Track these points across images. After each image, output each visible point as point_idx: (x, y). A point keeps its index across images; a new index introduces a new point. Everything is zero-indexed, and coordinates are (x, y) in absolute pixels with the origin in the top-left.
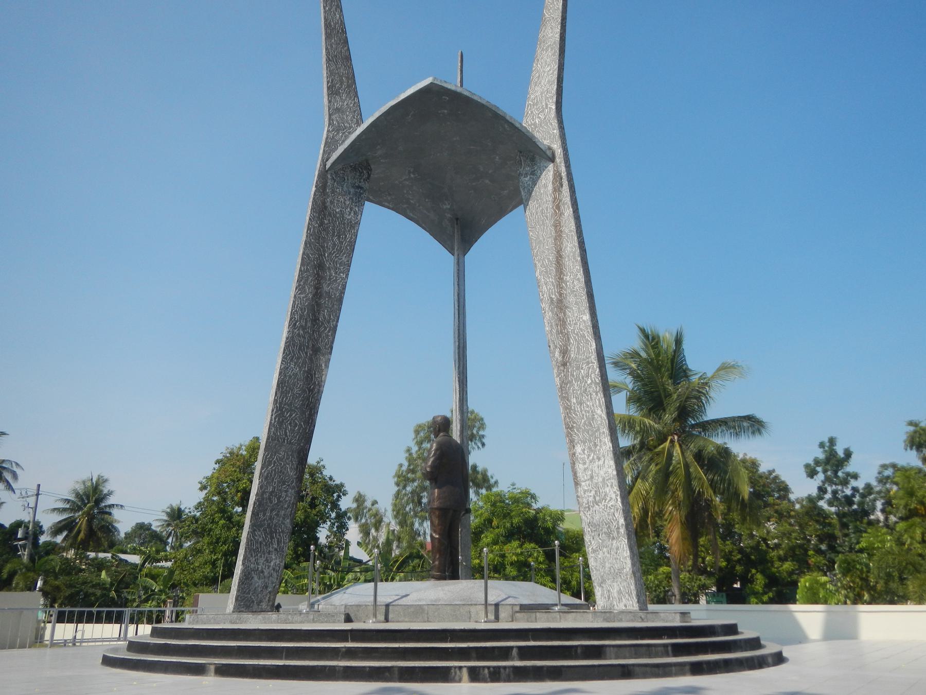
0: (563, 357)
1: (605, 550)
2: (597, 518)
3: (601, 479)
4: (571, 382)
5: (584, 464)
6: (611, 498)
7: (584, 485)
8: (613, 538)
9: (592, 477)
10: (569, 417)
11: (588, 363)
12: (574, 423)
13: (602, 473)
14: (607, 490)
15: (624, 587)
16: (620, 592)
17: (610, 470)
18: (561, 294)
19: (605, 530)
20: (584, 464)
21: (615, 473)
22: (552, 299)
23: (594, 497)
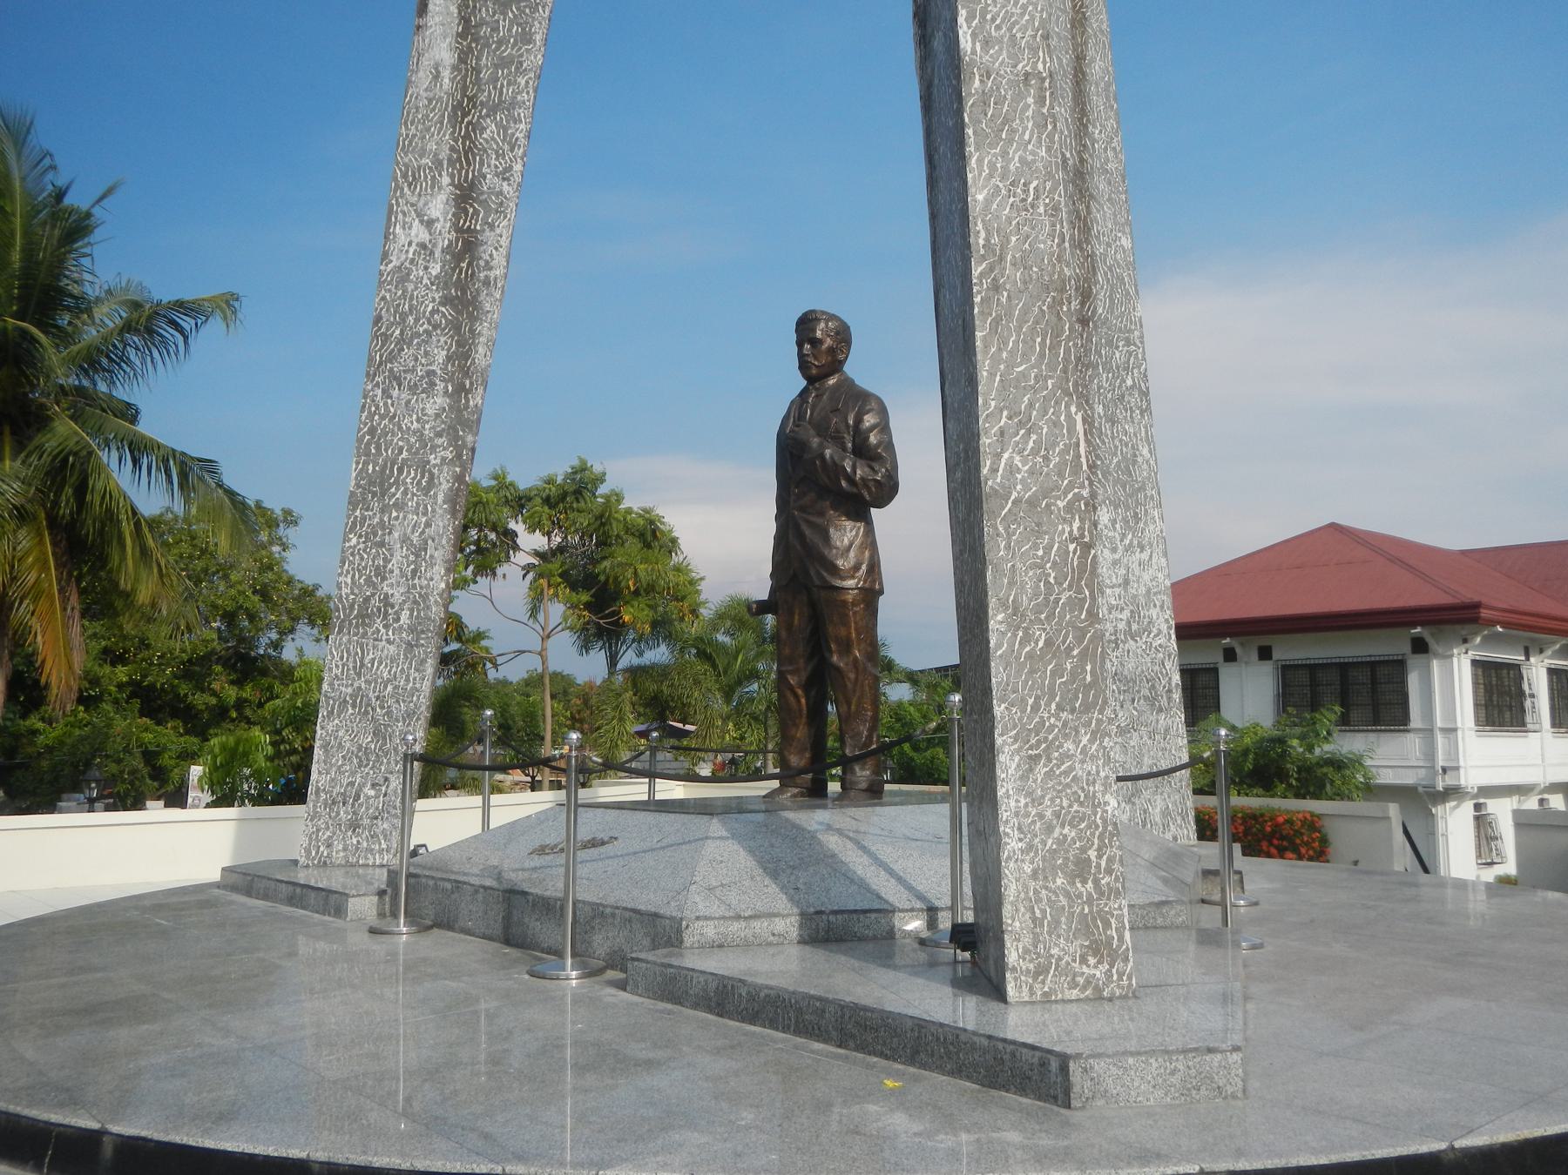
0: (1083, 304)
3: (1143, 590)
4: (1096, 367)
5: (1114, 550)
6: (1160, 632)
7: (1111, 596)
8: (1160, 710)
9: (1126, 582)
11: (1128, 343)
12: (1098, 457)
13: (1146, 577)
14: (1154, 612)
15: (1175, 803)
16: (1166, 813)
18: (1082, 161)
20: (1114, 550)
22: (1065, 160)
23: (1129, 623)
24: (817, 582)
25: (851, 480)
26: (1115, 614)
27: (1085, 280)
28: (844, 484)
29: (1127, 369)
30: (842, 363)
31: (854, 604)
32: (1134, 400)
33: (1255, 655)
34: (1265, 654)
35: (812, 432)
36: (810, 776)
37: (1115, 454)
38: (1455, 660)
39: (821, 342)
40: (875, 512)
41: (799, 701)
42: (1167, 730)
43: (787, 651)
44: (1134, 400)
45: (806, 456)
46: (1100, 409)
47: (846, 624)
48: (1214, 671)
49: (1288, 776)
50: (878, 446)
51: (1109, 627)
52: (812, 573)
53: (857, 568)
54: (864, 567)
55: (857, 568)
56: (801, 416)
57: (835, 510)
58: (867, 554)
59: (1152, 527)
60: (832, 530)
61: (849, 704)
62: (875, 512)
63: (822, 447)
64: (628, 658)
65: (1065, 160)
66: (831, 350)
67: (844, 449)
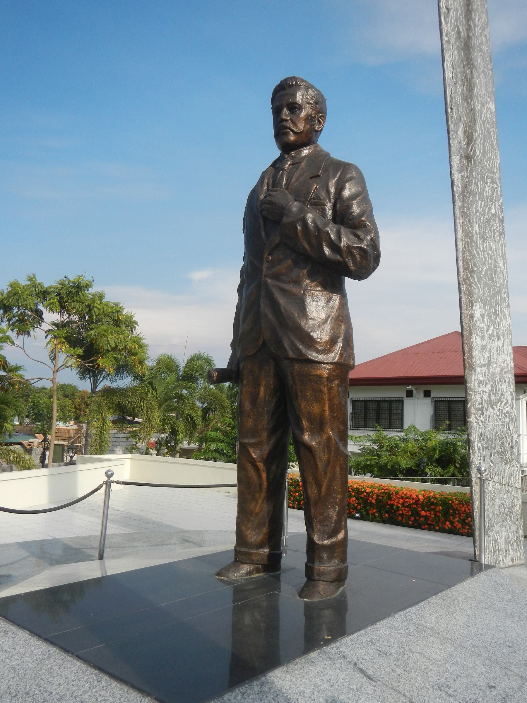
0: (468, 144)
1: (496, 478)
2: (490, 428)
3: (498, 370)
4: (475, 195)
8: (507, 462)
9: (489, 363)
10: (470, 252)
11: (493, 182)
12: (475, 264)
13: (501, 360)
14: (504, 386)
15: (513, 533)
16: (508, 541)
17: (508, 359)
18: (468, 37)
19: (498, 448)
20: (483, 338)
21: (512, 365)
22: (459, 33)
23: (490, 394)
24: (291, 354)
25: (335, 247)
26: (482, 388)
27: (470, 127)
28: (327, 251)
29: (492, 200)
30: (318, 132)
31: (329, 379)
32: (495, 224)
33: (422, 394)
34: (427, 394)
35: (290, 196)
36: (266, 550)
37: (484, 264)
38: (520, 401)
39: (300, 108)
40: (348, 282)
41: (260, 476)
42: (510, 477)
43: (250, 423)
44: (495, 224)
45: (285, 220)
46: (476, 228)
47: (319, 400)
48: (402, 402)
49: (455, 462)
50: (361, 215)
51: (478, 397)
52: (286, 344)
53: (333, 341)
54: (340, 345)
55: (333, 341)
56: (275, 183)
57: (311, 276)
58: (343, 328)
59: (504, 322)
60: (308, 300)
61: (319, 486)
62: (348, 282)
63: (302, 211)
64: (104, 384)
65: (459, 33)
66: (309, 119)
67: (323, 214)
